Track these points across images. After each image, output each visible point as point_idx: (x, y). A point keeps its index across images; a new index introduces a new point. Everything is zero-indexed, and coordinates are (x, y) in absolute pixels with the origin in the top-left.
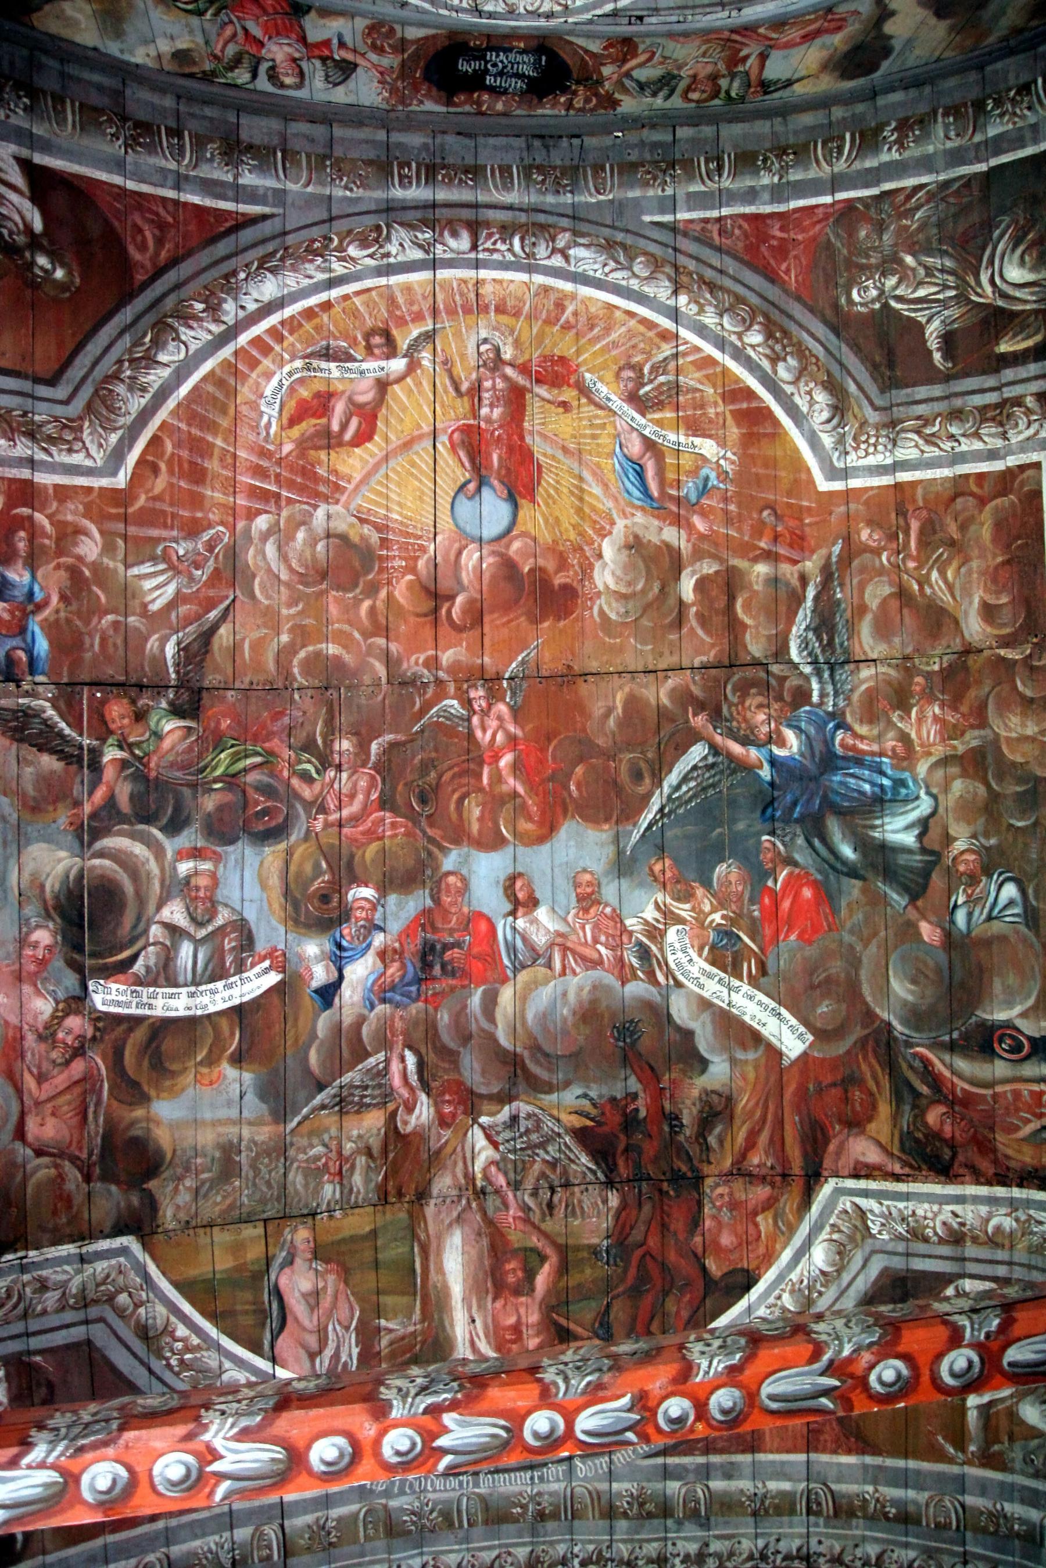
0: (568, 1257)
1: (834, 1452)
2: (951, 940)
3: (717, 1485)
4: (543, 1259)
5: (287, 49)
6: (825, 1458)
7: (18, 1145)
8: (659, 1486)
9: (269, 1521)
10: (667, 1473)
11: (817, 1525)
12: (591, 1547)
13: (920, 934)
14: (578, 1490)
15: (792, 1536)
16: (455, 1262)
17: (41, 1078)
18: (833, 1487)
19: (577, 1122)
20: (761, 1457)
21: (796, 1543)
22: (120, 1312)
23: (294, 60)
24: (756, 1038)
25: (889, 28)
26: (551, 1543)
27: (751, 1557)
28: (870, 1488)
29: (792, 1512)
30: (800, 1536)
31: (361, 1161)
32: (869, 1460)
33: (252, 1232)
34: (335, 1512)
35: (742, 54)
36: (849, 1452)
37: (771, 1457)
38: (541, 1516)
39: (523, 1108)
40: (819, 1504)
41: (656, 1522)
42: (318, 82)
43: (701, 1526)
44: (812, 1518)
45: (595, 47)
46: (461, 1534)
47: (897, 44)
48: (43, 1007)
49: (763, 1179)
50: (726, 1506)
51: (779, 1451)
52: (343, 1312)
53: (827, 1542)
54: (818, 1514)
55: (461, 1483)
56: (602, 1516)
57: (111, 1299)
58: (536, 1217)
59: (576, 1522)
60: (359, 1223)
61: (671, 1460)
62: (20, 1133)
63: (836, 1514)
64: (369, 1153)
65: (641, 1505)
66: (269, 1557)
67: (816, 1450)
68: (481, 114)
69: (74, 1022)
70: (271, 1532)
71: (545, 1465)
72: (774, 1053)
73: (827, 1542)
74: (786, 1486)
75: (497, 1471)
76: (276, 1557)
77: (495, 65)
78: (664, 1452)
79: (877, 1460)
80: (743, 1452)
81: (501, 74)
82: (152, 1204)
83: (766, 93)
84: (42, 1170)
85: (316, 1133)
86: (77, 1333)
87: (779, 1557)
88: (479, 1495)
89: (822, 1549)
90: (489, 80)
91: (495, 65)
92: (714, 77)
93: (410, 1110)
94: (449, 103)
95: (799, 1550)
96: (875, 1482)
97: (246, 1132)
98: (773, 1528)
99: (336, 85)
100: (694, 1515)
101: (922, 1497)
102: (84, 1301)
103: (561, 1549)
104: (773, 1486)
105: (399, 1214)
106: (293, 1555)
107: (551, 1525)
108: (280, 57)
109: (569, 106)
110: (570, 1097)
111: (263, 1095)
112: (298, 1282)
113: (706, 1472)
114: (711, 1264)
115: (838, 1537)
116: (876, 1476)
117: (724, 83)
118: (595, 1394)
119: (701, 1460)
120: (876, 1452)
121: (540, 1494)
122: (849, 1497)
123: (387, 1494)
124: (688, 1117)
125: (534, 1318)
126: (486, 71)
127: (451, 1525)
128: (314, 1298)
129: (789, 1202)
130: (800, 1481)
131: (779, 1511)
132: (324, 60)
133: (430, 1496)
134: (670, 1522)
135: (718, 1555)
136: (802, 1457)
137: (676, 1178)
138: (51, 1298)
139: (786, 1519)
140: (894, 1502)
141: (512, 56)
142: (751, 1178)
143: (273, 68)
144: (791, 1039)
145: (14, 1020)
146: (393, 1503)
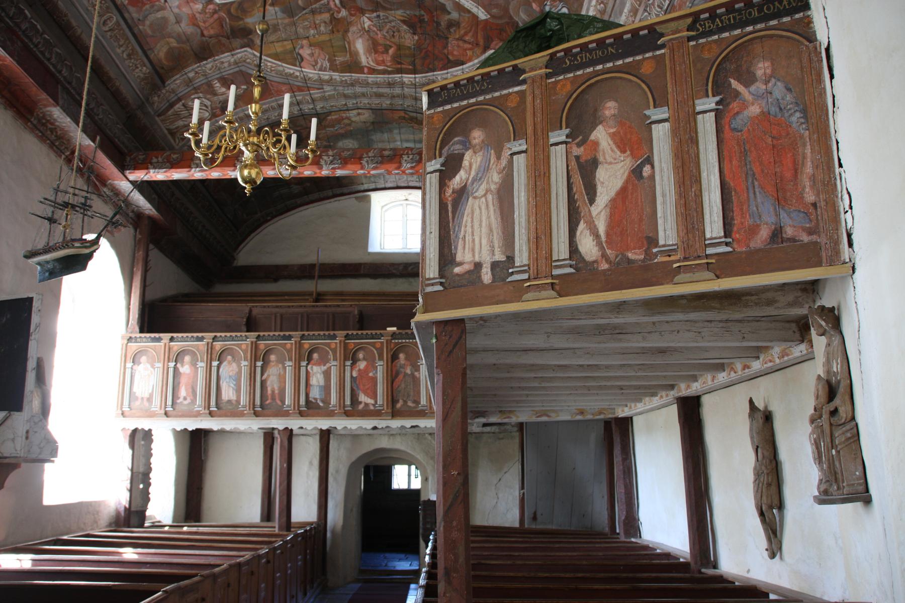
0: (399, 47)
2: (542, 11)
4: (391, 47)
7: (204, 39)
13: (532, 7)
16: (360, 46)
17: (204, 22)
19: (402, 18)
22: (249, 63)
24: (469, 11)
31: (323, 25)
33: (286, 43)
39: (381, 14)
48: (199, 7)
49: (470, 43)
52: (323, 56)
57: (245, 61)
58: (388, 37)
60: (326, 38)
62: (203, 35)
64: (325, 22)
69: (211, 7)
70: (308, 98)
72: (475, 17)
82: (252, 41)
84: (213, 41)
85: (306, 19)
86: (237, 69)
93: (339, 12)
97: (280, 21)
102: (236, 63)
105: (340, 35)
110: (400, 12)
111: (283, 12)
112: (305, 52)
114: (451, 57)
118: (374, 168)
124: (443, 24)
125: (389, 59)
128: (312, 55)
129: (478, 50)
137: (438, 36)
138: (226, 65)
142: (465, 42)
144: (482, 15)
145: (190, 12)
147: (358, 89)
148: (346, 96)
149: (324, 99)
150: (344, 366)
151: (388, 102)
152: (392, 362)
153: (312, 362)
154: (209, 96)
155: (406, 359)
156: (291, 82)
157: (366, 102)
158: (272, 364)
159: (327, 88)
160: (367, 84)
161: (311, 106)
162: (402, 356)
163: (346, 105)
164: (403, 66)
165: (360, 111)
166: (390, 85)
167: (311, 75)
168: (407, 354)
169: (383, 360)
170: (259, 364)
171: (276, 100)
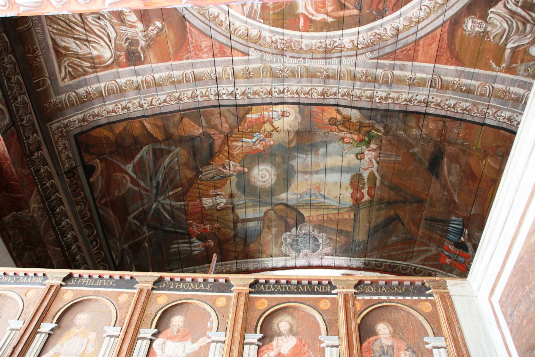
1: (446, 64)
3: (397, 72)
6: (441, 66)
8: (374, 70)
9: (229, 65)
10: (377, 66)
11: (433, 91)
12: (345, 90)
14: (343, 69)
15: (423, 95)
18: (442, 77)
20: (415, 63)
21: (424, 97)
26: (331, 87)
27: (405, 100)
28: (457, 79)
29: (424, 86)
30: (426, 95)
32: (459, 68)
34: (252, 66)
36: (452, 64)
37: (419, 64)
38: (328, 77)
40: (436, 84)
41: (371, 84)
43: (388, 87)
44: (431, 89)
46: (298, 80)
50: (399, 81)
51: (423, 62)
53: (435, 98)
54: (434, 87)
55: (299, 61)
56: (351, 79)
59: (341, 81)
61: (379, 61)
63: (441, 88)
65: (366, 77)
66: (229, 78)
67: (439, 63)
70: (229, 70)
71: (331, 58)
73: (435, 98)
74: (424, 76)
75: (312, 58)
76: (231, 78)
78: (378, 58)
79: (463, 69)
80: (409, 61)
87: (416, 102)
88: (305, 67)
89: (433, 100)
95: (424, 100)
96: (460, 77)
98: (416, 90)
100: (386, 83)
101: (477, 83)
103: (335, 90)
104: (419, 75)
106: (237, 79)
107: (331, 81)
113: (393, 67)
115: (440, 96)
116: (460, 74)
119: (392, 62)
120: (463, 65)
121: (328, 69)
122: (448, 82)
123: (271, 62)
127: (294, 76)
130: (430, 74)
131: (419, 85)
133: (287, 65)
134: (376, 85)
135: (393, 99)
136: (433, 65)
139: (421, 88)
140: (465, 85)
146: (273, 66)
147: (290, 63)
148: (274, 75)
149: (248, 75)
150: (243, 344)
151: (320, 89)
152: (361, 343)
153: (167, 333)
154: (115, 21)
155: (394, 335)
156: (214, 34)
157: (294, 89)
158: (74, 330)
159: (254, 55)
160: (299, 52)
161: (231, 89)
162: (383, 329)
163: (270, 93)
164: (347, 12)
165: (285, 108)
166: (327, 52)
167: (237, 24)
168: (393, 324)
169: (337, 333)
170: (46, 327)
171: (193, 66)
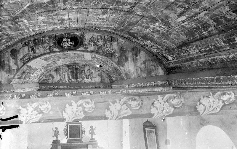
5: (99, 44)
23: (98, 42)
25: (14, 61)
35: (33, 51)
42: (95, 37)
45: (55, 49)
47: (11, 58)
68: (70, 33)
77: (69, 43)
81: (68, 42)
83: (25, 43)
90: (69, 40)
91: (69, 43)
92: (35, 45)
94: (75, 34)
99: (92, 37)
108: (100, 42)
109: (56, 36)
117: (33, 45)
126: (70, 42)
132: (94, 42)
141: (67, 46)
143: (102, 40)
